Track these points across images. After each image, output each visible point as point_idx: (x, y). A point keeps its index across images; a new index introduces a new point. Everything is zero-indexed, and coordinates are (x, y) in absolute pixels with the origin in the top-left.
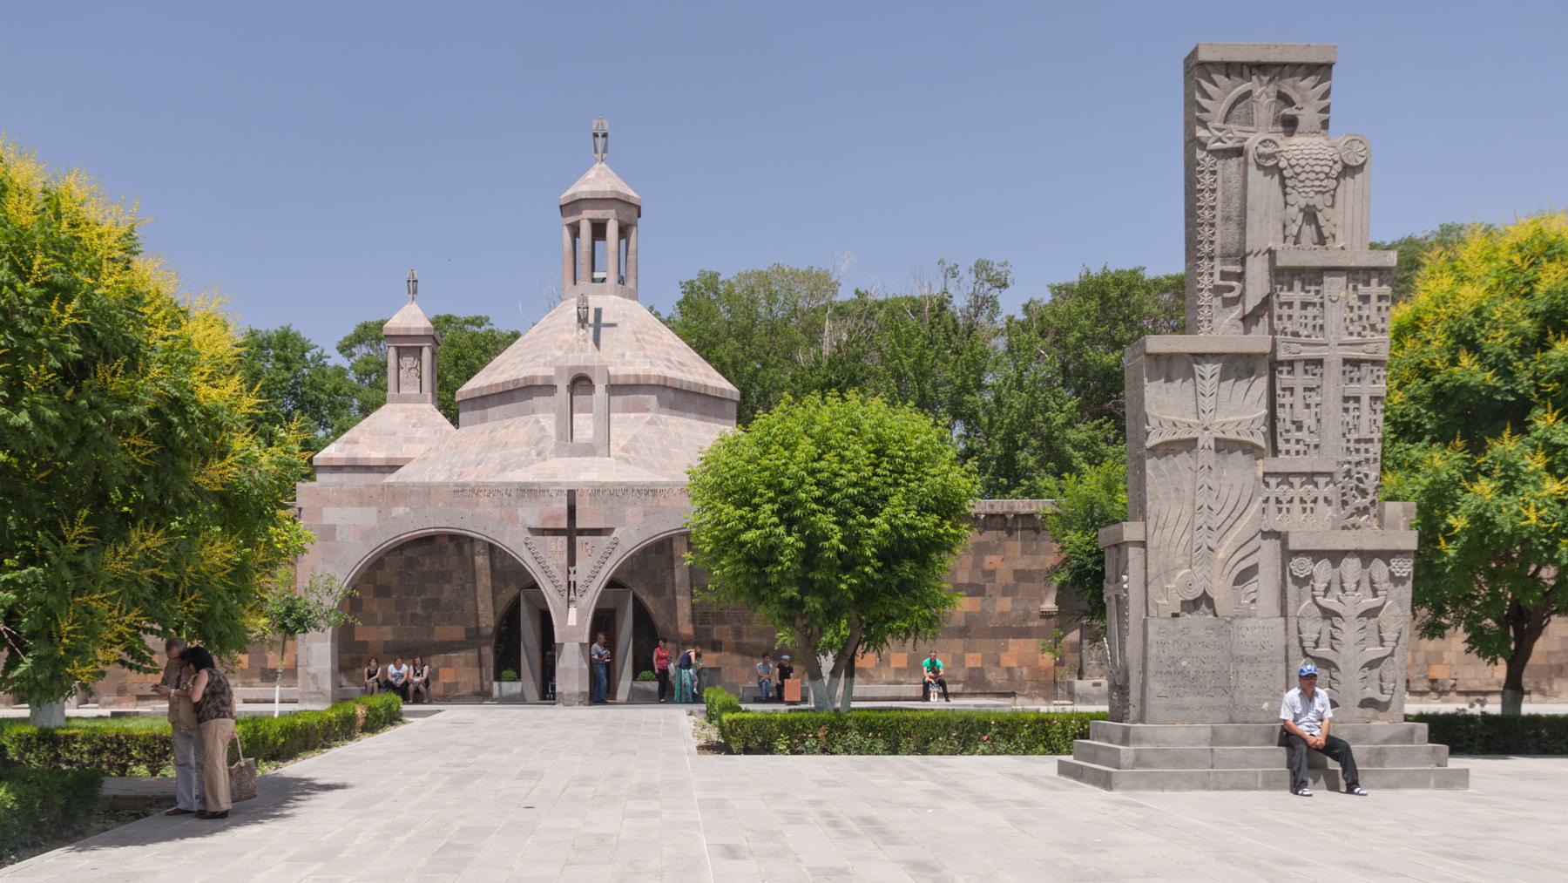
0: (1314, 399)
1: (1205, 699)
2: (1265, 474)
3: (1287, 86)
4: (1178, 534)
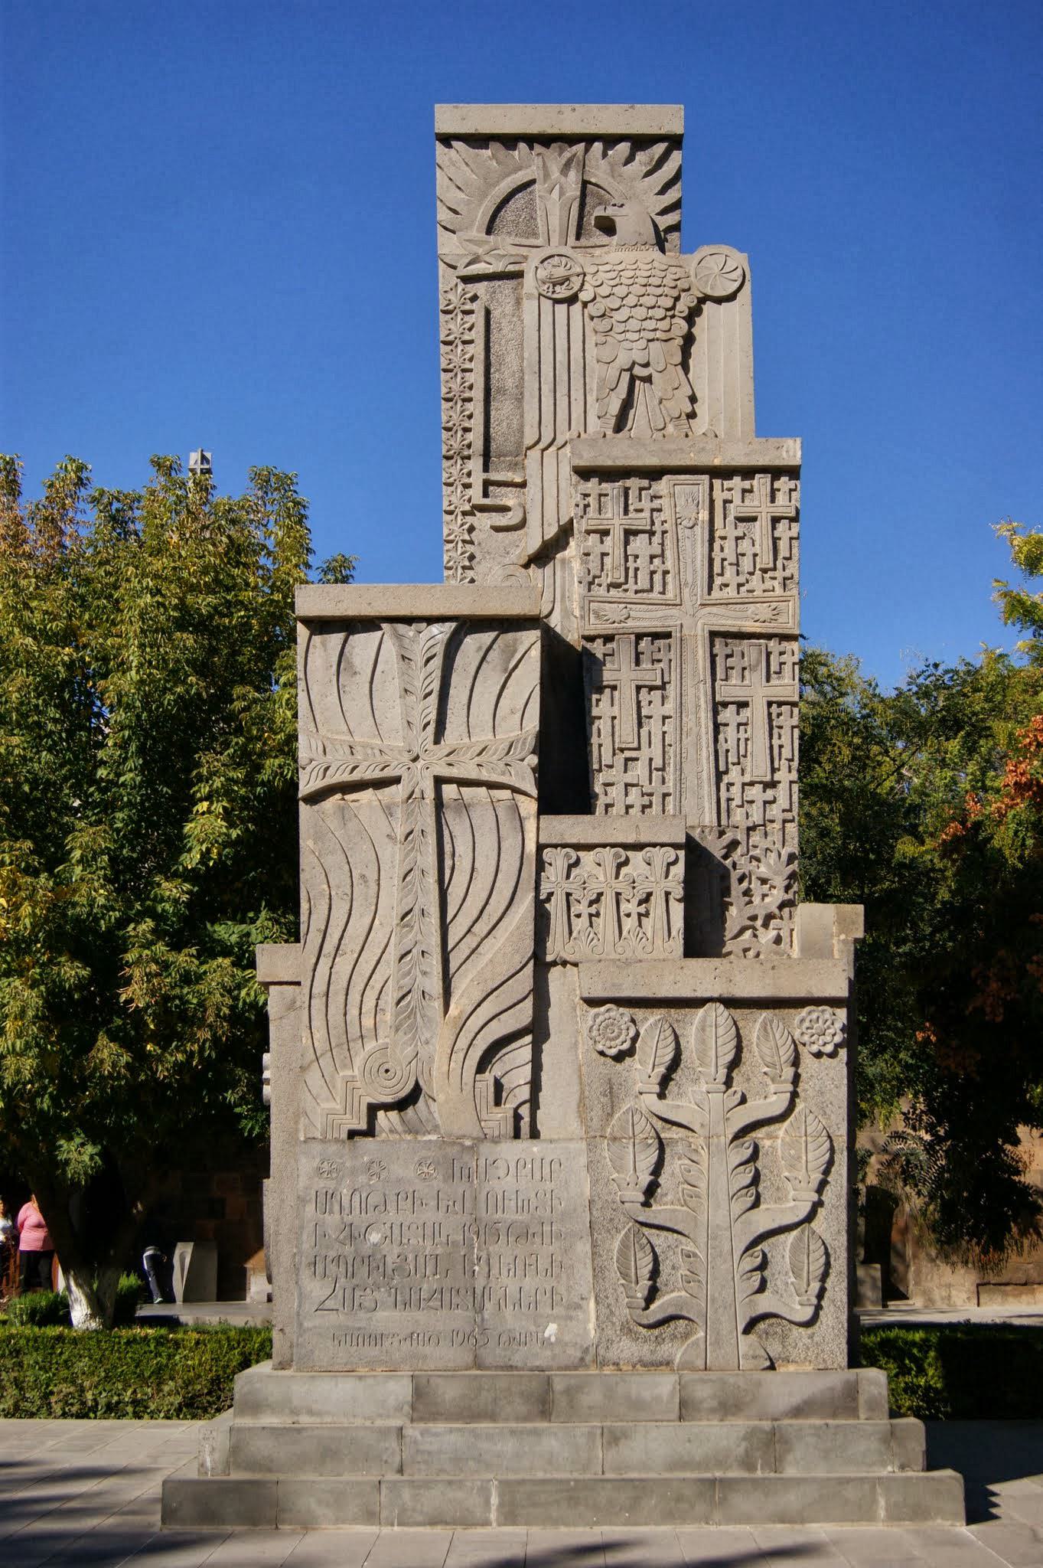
0: (654, 707)
1: (421, 1316)
2: (540, 848)
3: (600, 166)
4: (365, 967)
